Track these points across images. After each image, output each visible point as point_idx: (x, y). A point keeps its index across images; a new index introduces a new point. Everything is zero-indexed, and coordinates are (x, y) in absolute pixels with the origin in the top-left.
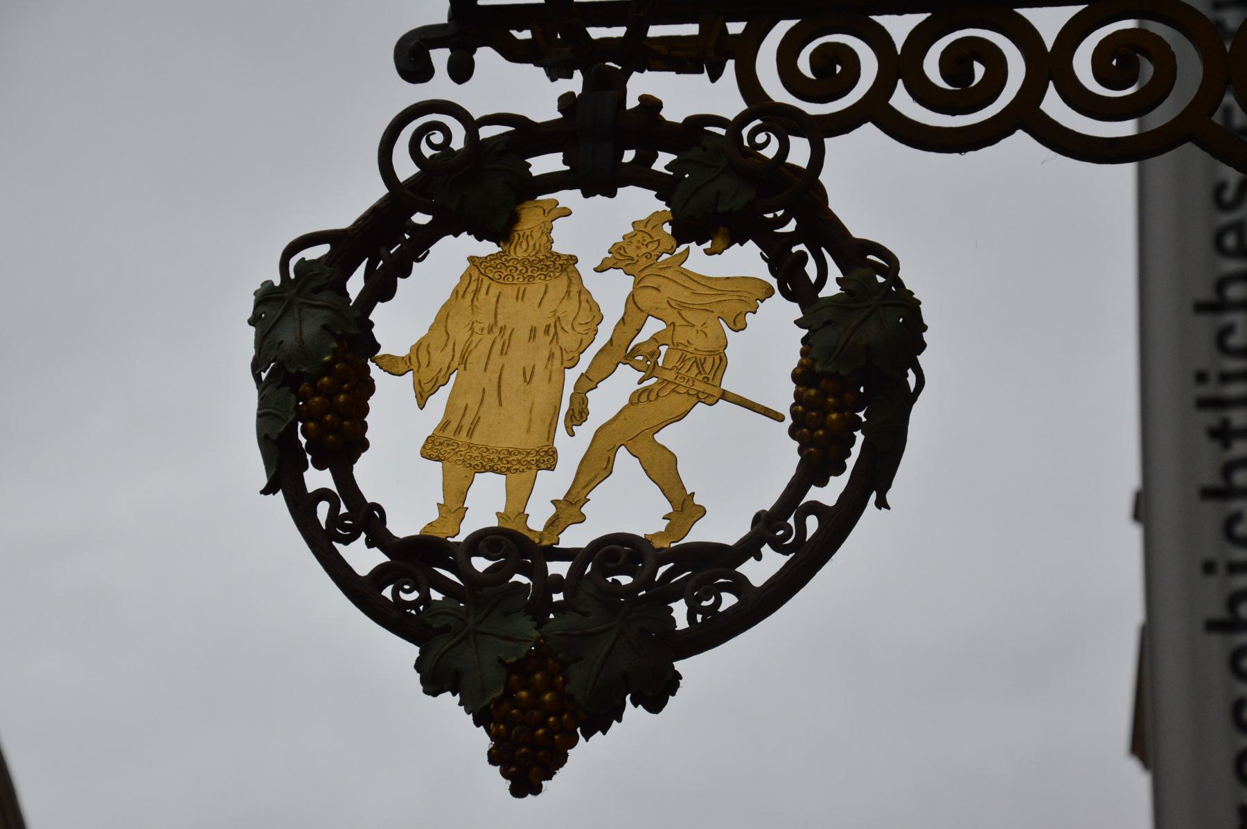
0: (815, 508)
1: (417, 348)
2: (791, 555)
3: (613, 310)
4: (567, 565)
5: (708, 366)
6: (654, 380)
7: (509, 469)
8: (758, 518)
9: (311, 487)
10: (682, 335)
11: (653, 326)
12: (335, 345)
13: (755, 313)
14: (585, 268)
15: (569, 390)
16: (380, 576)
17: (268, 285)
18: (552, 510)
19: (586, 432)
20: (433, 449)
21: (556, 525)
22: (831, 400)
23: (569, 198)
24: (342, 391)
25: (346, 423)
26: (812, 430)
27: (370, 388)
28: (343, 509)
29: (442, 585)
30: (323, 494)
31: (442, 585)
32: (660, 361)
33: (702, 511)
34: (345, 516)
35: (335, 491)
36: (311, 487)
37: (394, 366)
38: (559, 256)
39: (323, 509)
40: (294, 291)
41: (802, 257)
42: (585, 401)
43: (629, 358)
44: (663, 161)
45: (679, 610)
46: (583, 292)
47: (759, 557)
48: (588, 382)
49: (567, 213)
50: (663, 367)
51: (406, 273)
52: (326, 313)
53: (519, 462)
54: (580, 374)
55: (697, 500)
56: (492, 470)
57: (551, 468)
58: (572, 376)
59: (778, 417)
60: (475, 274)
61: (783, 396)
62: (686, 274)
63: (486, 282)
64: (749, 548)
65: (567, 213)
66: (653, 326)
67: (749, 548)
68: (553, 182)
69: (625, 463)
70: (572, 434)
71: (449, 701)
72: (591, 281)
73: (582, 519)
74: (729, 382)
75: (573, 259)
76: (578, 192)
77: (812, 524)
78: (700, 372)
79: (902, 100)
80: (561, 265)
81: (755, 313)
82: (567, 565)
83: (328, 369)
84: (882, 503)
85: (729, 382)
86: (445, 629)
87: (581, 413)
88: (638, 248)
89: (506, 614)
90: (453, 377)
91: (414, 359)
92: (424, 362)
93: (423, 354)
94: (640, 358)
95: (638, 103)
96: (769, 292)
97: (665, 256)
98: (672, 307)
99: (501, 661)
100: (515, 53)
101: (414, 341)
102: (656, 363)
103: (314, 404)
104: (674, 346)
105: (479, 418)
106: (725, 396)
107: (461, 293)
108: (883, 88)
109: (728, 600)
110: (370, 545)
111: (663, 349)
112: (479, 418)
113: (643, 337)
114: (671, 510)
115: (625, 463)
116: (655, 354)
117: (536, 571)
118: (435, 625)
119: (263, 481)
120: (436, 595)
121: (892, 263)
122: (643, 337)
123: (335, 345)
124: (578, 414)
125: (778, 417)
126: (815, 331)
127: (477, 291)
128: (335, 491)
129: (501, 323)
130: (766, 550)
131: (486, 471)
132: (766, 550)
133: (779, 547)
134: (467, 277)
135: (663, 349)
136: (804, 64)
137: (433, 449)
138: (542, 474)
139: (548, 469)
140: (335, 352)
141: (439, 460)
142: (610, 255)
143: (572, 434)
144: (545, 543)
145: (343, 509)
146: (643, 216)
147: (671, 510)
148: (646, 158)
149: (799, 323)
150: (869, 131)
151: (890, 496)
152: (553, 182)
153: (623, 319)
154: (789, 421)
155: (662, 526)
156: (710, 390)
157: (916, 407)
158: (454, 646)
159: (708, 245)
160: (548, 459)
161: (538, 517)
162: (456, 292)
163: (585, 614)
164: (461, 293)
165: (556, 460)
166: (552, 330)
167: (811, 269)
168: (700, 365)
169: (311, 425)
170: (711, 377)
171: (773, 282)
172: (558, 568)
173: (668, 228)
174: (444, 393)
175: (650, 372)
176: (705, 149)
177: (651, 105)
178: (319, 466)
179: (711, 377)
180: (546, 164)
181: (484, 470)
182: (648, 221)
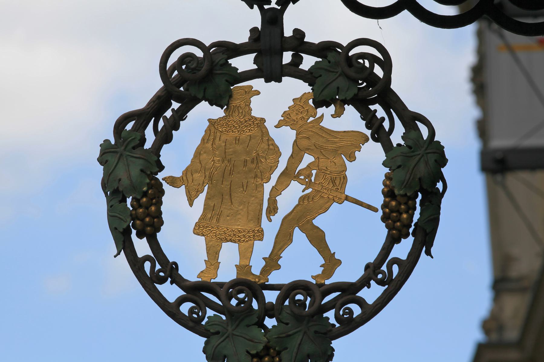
0: (396, 261)
1: (186, 172)
2: (387, 286)
3: (286, 152)
5: (337, 182)
6: (310, 190)
7: (239, 240)
8: (367, 267)
9: (140, 255)
10: (323, 163)
11: (308, 159)
12: (148, 181)
13: (359, 151)
14: (270, 125)
15: (266, 196)
16: (181, 301)
17: (107, 141)
18: (263, 263)
19: (278, 219)
20: (199, 229)
21: (266, 271)
22: (403, 207)
23: (258, 83)
24: (152, 205)
25: (155, 220)
26: (394, 222)
27: (162, 192)
28: (158, 267)
29: (213, 306)
30: (147, 258)
31: (213, 306)
32: (313, 179)
33: (339, 262)
34: (160, 271)
35: (153, 256)
36: (140, 255)
37: (173, 181)
38: (256, 119)
39: (147, 266)
40: (123, 148)
41: (383, 119)
42: (275, 202)
43: (296, 178)
45: (330, 315)
46: (270, 139)
47: (369, 287)
48: (276, 191)
49: (258, 93)
50: (314, 183)
52: (141, 161)
53: (244, 236)
54: (272, 187)
55: (337, 257)
56: (231, 241)
57: (261, 239)
58: (268, 187)
59: (376, 210)
60: (213, 130)
61: (378, 200)
62: (322, 128)
63: (218, 134)
64: (364, 282)
65: (258, 93)
66: (308, 159)
67: (364, 282)
68: (249, 75)
69: (299, 236)
70: (270, 220)
72: (273, 133)
73: (278, 267)
74: (349, 191)
75: (263, 120)
76: (262, 80)
77: (396, 269)
78: (334, 186)
80: (257, 124)
81: (359, 151)
83: (145, 194)
84: (428, 253)
85: (349, 191)
86: (218, 333)
87: (274, 209)
88: (297, 114)
89: (248, 326)
90: (206, 188)
91: (184, 178)
92: (190, 180)
93: (189, 175)
94: (302, 177)
95: (291, 34)
96: (367, 140)
97: (311, 119)
98: (317, 148)
99: (248, 352)
101: (184, 169)
102: (311, 180)
103: (139, 212)
104: (319, 170)
105: (222, 211)
106: (347, 198)
107: (206, 141)
109: (357, 310)
110: (172, 283)
111: (314, 172)
112: (222, 211)
113: (303, 165)
114: (324, 262)
115: (299, 236)
116: (310, 175)
118: (212, 331)
119: (116, 252)
122: (303, 165)
123: (148, 181)
124: (273, 209)
125: (376, 210)
126: (394, 170)
127: (214, 139)
128: (153, 256)
129: (228, 157)
130: (372, 282)
131: (228, 241)
132: (372, 282)
133: (380, 283)
134: (208, 131)
135: (314, 172)
137: (199, 229)
138: (257, 243)
139: (259, 240)
140: (148, 184)
141: (203, 235)
142: (282, 118)
143: (270, 220)
144: (262, 281)
145: (158, 267)
146: (298, 96)
147: (324, 262)
148: (297, 60)
149: (385, 164)
151: (433, 250)
152: (249, 75)
153: (292, 155)
154: (380, 213)
155: (319, 271)
156: (339, 195)
157: (443, 200)
158: (222, 341)
159: (332, 107)
160: (259, 235)
161: (256, 270)
162: (203, 139)
163: (287, 324)
164: (206, 141)
165: (263, 235)
166: (255, 162)
168: (333, 181)
169: (138, 222)
170: (339, 188)
171: (368, 133)
172: (271, 296)
173: (311, 102)
174: (202, 197)
175: (309, 185)
176: (329, 62)
178: (140, 235)
179: (339, 188)
181: (227, 241)
182: (301, 98)
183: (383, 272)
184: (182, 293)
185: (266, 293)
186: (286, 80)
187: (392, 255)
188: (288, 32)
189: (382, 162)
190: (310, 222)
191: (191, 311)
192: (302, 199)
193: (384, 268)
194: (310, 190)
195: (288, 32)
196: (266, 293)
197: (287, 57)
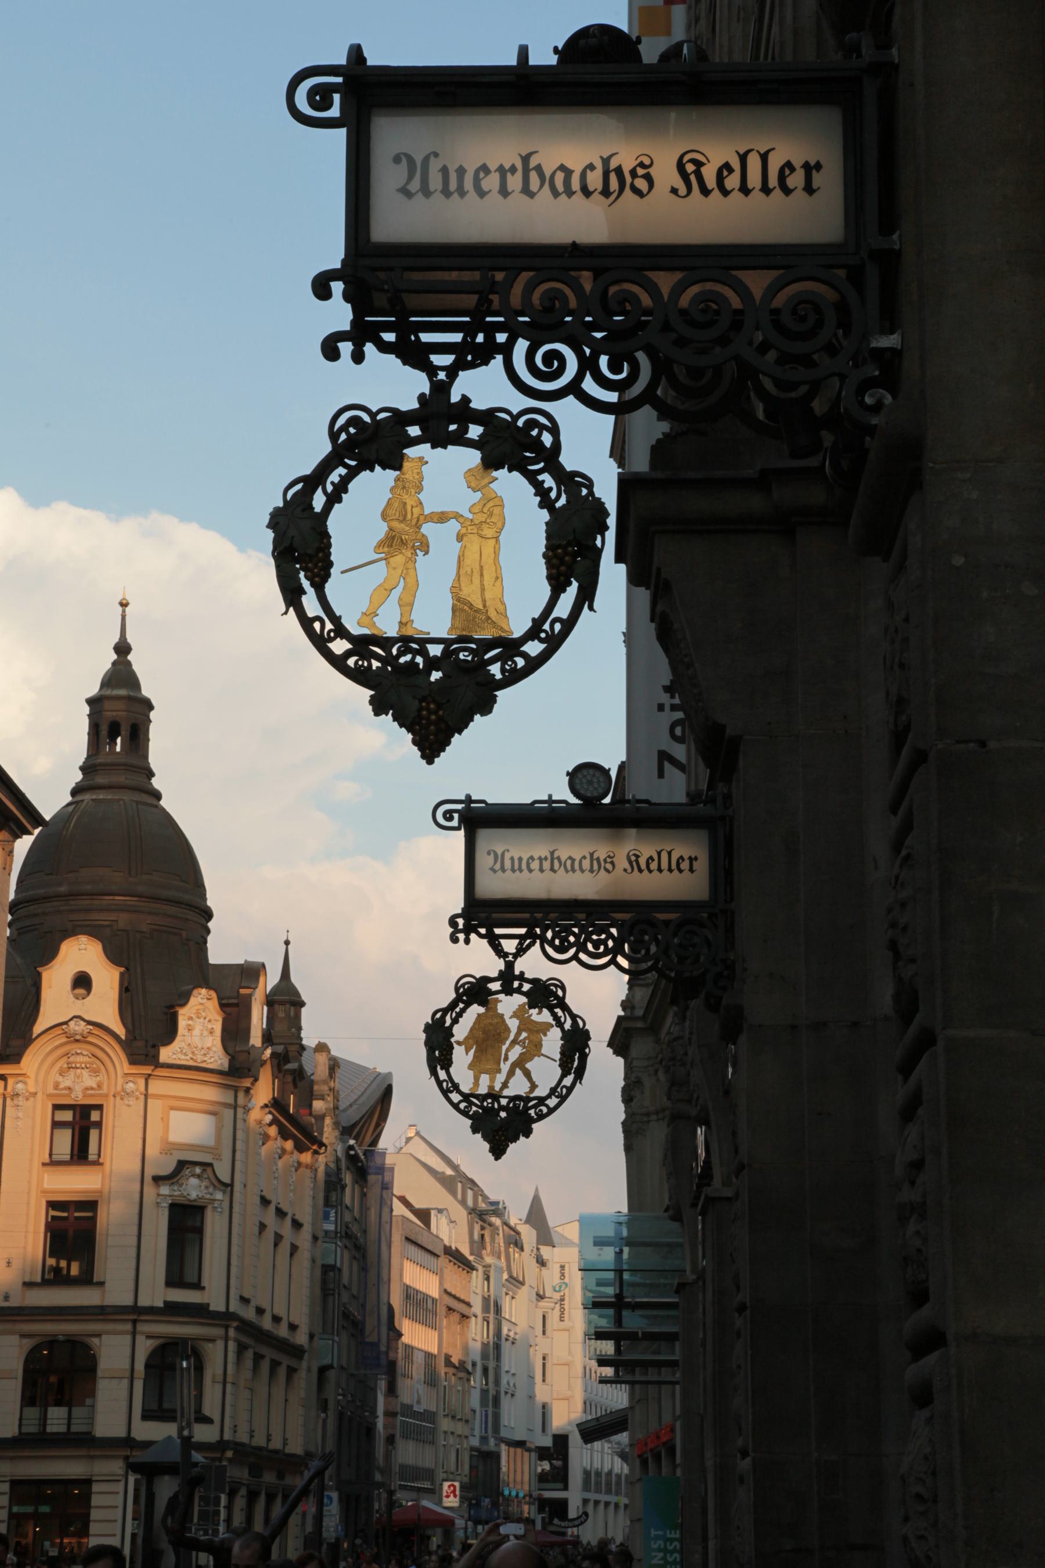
0: (557, 620)
4: (441, 647)
16: (348, 654)
29: (378, 657)
31: (378, 657)
44: (475, 431)
51: (346, 491)
71: (387, 719)
77: (558, 627)
79: (589, 385)
82: (441, 647)
100: (384, 348)
108: (579, 377)
117: (424, 652)
120: (375, 664)
121: (590, 484)
136: (538, 360)
150: (571, 399)
167: (553, 495)
172: (435, 650)
177: (465, 400)
180: (414, 431)
183: (545, 631)
184: (349, 646)
185: (429, 646)
186: (515, 995)
187: (553, 615)
188: (517, 972)
189: (545, 535)
190: (524, 1066)
191: (356, 663)
192: (521, 1054)
193: (546, 627)
194: (525, 1050)
195: (517, 972)
196: (429, 646)
197: (516, 984)
